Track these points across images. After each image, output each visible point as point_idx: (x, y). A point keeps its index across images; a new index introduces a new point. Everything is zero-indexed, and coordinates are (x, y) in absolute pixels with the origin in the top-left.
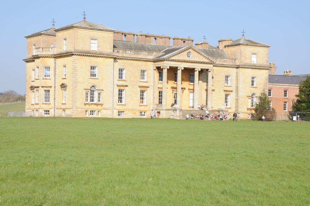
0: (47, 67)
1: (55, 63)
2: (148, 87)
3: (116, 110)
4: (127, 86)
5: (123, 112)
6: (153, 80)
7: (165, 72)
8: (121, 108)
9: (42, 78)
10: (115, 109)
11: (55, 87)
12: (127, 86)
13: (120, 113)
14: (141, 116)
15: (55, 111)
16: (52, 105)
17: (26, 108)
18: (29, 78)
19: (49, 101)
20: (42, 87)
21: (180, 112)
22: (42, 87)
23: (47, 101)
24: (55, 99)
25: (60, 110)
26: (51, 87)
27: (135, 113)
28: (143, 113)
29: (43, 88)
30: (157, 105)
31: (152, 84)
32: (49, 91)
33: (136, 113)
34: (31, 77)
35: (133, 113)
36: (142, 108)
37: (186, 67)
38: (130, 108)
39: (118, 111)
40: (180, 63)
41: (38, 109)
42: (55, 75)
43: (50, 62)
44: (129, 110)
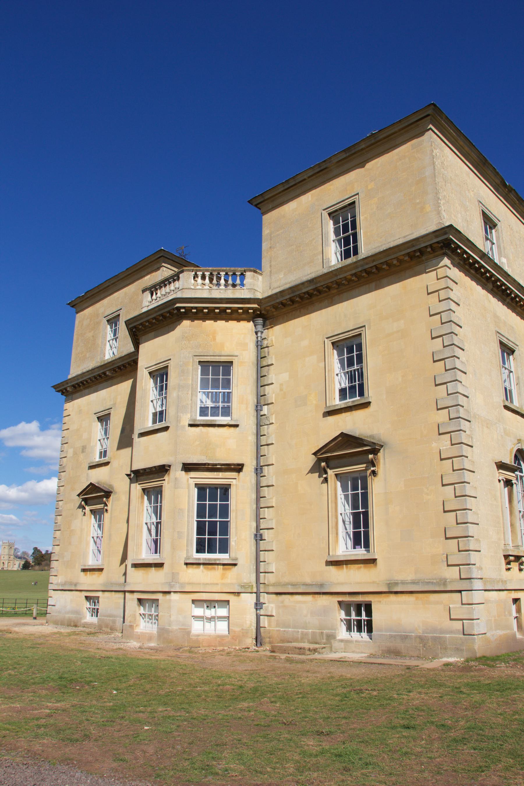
0: (216, 364)
1: (260, 346)
9: (186, 420)
11: (259, 470)
15: (258, 605)
16: (245, 573)
17: (51, 587)
18: (75, 453)
19: (224, 548)
20: (188, 467)
22: (188, 467)
23: (211, 550)
24: (258, 537)
25: (309, 598)
26: (238, 468)
29: (193, 474)
32: (225, 489)
34: (84, 449)
41: (159, 596)
42: (258, 408)
43: (234, 338)
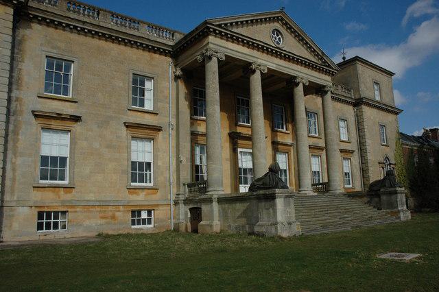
2: (159, 129)
3: (26, 210)
4: (76, 119)
5: (64, 213)
6: (175, 110)
7: (212, 70)
8: (50, 200)
10: (21, 203)
12: (76, 119)
13: (46, 218)
14: (136, 226)
21: (287, 204)
27: (113, 217)
28: (144, 215)
30: (189, 186)
31: (173, 122)
33: (118, 214)
35: (102, 218)
36: (140, 198)
37: (273, 67)
38: (91, 197)
39: (35, 212)
40: (255, 53)
44: (88, 206)
